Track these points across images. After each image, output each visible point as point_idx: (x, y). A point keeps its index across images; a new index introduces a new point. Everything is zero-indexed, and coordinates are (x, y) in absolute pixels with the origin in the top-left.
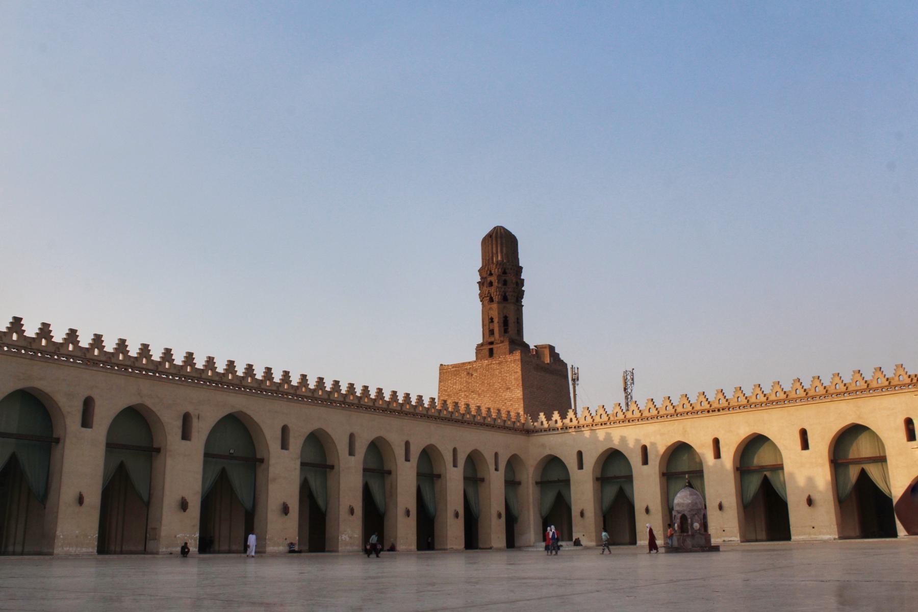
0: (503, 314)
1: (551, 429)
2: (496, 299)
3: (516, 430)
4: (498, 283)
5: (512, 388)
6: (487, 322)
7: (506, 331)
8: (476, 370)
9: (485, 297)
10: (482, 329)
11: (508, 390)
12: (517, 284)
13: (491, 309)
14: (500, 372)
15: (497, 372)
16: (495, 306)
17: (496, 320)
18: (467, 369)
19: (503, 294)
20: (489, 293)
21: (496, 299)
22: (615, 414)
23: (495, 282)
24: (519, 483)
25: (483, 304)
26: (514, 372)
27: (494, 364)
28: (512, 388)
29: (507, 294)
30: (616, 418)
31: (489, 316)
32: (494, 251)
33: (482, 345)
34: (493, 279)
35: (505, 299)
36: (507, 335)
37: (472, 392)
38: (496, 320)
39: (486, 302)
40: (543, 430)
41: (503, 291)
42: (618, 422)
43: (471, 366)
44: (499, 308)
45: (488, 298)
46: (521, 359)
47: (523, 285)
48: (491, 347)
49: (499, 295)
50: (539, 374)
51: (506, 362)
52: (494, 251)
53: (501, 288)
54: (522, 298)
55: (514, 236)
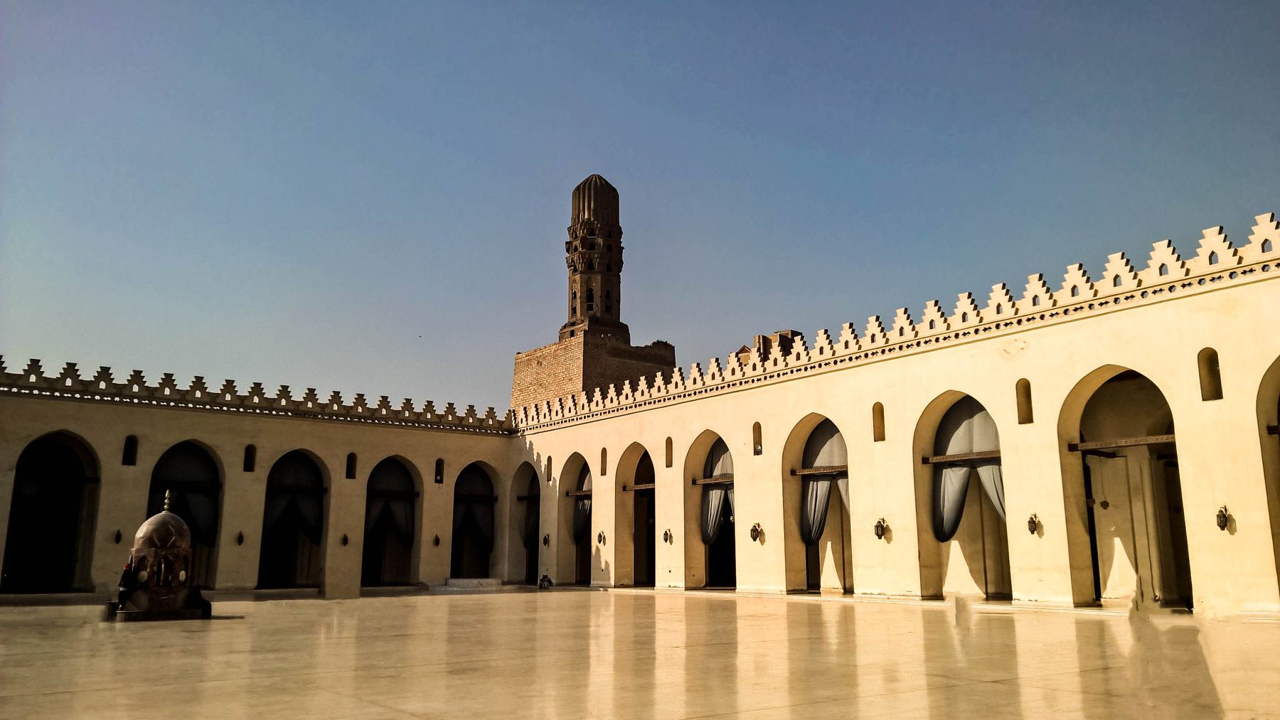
2: (579, 267)
7: (590, 308)
8: (545, 358)
16: (578, 277)
17: (578, 295)
20: (573, 261)
21: (579, 267)
24: (496, 499)
32: (581, 208)
34: (577, 243)
35: (589, 267)
37: (541, 385)
38: (578, 295)
44: (581, 278)
48: (572, 328)
50: (617, 359)
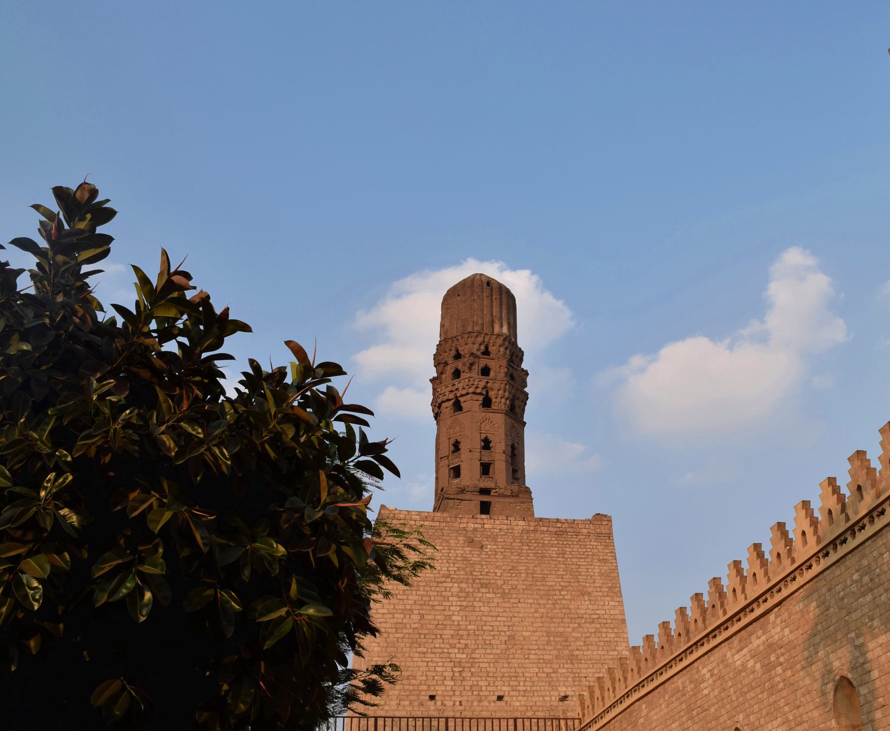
5: (595, 594)
8: (494, 539)
9: (474, 393)
11: (586, 598)
15: (553, 551)
18: (464, 529)
20: (485, 387)
26: (599, 560)
27: (543, 532)
28: (595, 594)
37: (483, 585)
43: (476, 526)
45: (481, 398)
48: (485, 498)
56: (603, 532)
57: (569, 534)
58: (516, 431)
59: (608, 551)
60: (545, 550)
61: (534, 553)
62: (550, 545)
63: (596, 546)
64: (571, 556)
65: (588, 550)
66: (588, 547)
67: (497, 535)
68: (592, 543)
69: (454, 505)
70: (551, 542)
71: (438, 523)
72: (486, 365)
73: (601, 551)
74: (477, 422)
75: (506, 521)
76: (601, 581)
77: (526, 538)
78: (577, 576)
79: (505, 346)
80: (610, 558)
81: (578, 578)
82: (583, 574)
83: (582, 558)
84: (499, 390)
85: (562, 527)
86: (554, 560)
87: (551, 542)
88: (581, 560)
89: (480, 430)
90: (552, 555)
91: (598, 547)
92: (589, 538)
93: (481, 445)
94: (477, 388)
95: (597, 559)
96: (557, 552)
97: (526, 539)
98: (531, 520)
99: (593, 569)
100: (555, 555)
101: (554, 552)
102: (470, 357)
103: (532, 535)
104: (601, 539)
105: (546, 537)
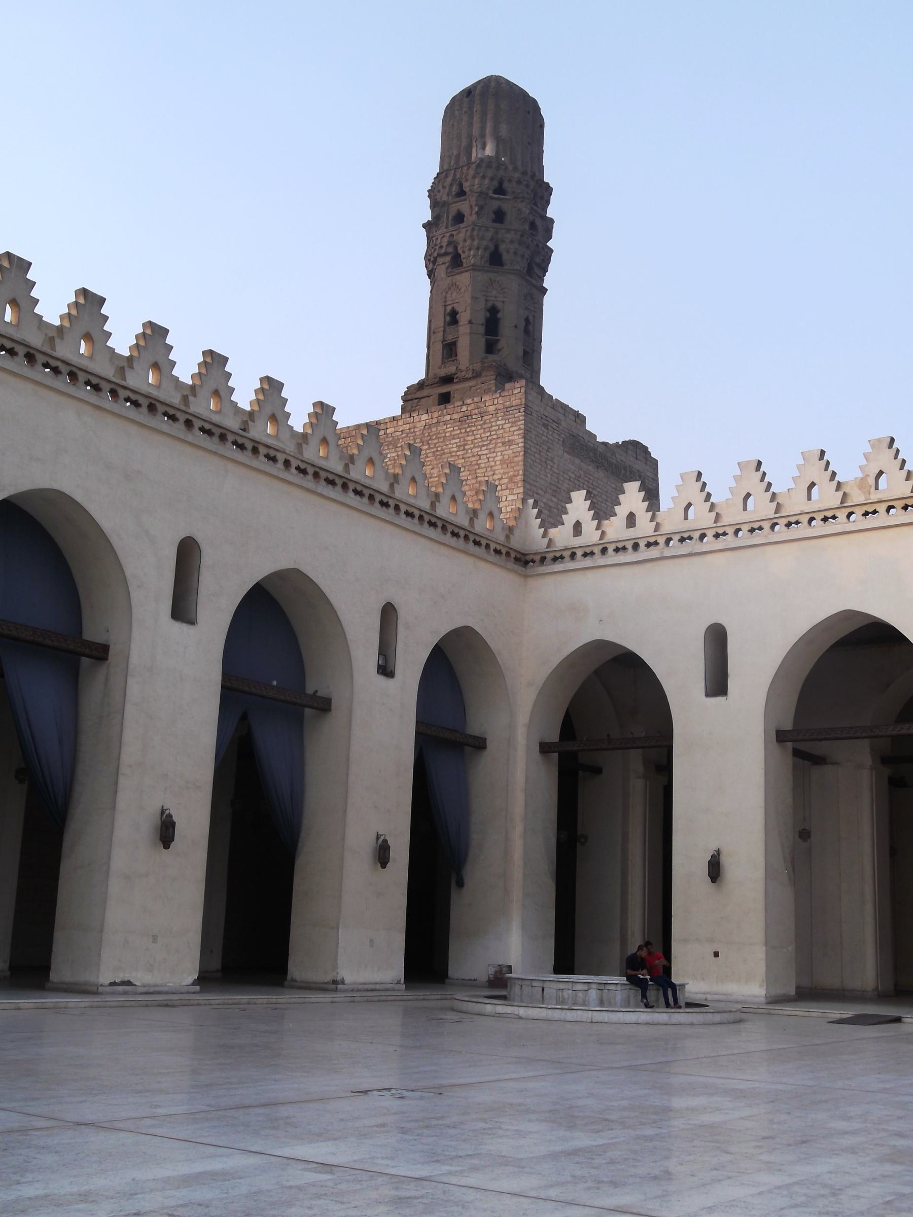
0: (486, 300)
1: (611, 548)
2: (470, 257)
3: (477, 543)
4: (477, 213)
6: (440, 322)
7: (490, 348)
9: (439, 255)
10: (426, 350)
12: (533, 225)
13: (454, 286)
14: (463, 446)
19: (492, 247)
20: (449, 243)
22: (871, 481)
23: (471, 215)
24: (480, 744)
25: (433, 284)
26: (504, 443)
27: (445, 423)
29: (502, 247)
30: (874, 497)
31: (445, 306)
32: (476, 132)
33: (421, 385)
35: (495, 259)
36: (491, 357)
38: (463, 318)
39: (441, 271)
40: (579, 553)
41: (492, 240)
42: (882, 508)
45: (448, 258)
46: (526, 406)
47: (550, 237)
48: (444, 389)
49: (478, 249)
50: (577, 461)
51: (482, 414)
52: (476, 132)
53: (487, 229)
54: (545, 270)
55: (535, 102)
56: (514, 404)
57: (474, 417)
58: (500, 286)
59: (515, 428)
60: (446, 445)
61: (434, 452)
62: (452, 436)
63: (503, 425)
64: (472, 446)
65: (492, 433)
66: (493, 428)
67: (398, 438)
68: (498, 423)
69: (412, 407)
70: (453, 433)
71: (344, 439)
72: (458, 210)
73: (507, 430)
74: (442, 293)
75: (408, 419)
76: (502, 471)
77: (427, 434)
78: (476, 470)
79: (482, 174)
80: (516, 437)
81: (476, 473)
82: (483, 465)
83: (484, 445)
84: (465, 241)
85: (467, 410)
86: (453, 456)
87: (453, 433)
88: (484, 448)
89: (445, 302)
90: (452, 450)
91: (505, 426)
92: (496, 417)
93: (445, 320)
94: (441, 247)
95: (500, 442)
96: (458, 444)
97: (427, 436)
98: (435, 410)
99: (494, 457)
100: (455, 449)
101: (455, 446)
102: (435, 209)
103: (434, 429)
104: (509, 415)
105: (449, 428)
